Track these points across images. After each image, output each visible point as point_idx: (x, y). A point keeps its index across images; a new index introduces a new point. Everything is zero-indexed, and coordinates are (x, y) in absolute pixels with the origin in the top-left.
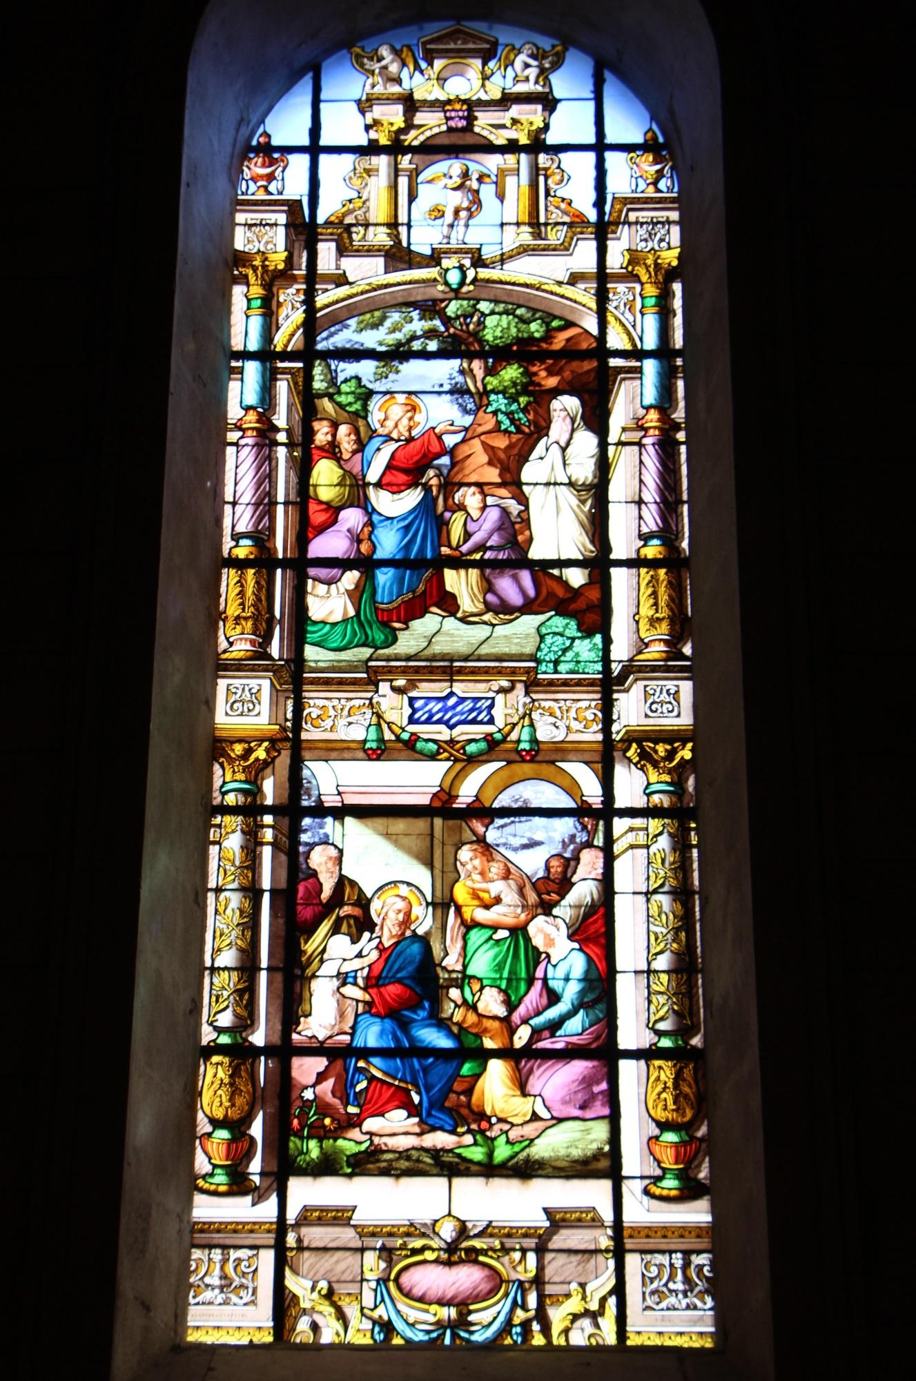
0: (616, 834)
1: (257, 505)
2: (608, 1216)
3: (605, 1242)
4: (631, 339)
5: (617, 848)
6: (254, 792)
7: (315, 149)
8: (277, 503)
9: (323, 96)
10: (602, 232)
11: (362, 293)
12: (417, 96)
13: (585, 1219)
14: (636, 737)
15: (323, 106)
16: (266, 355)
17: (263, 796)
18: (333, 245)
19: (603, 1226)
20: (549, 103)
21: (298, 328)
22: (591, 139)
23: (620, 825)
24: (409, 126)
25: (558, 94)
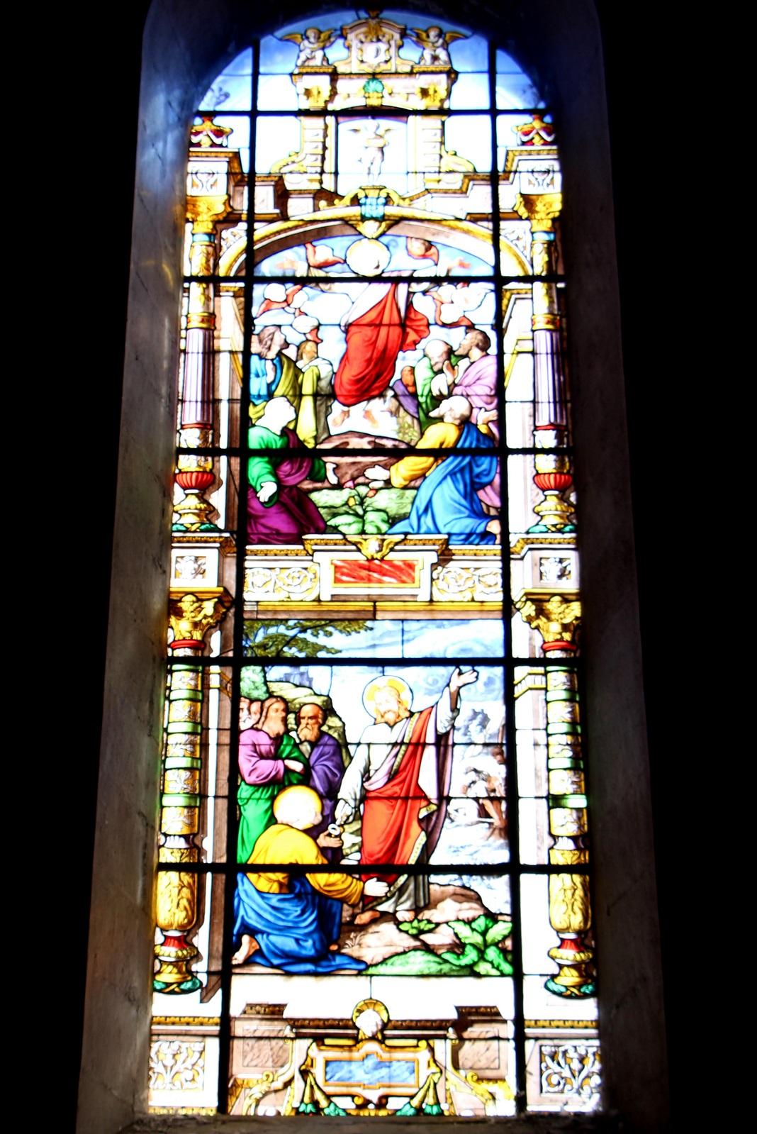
0: (517, 678)
1: (203, 402)
2: (508, 1012)
3: (509, 1030)
4: (521, 263)
5: (517, 691)
6: (202, 645)
7: (254, 114)
8: (219, 401)
9: (262, 70)
10: (494, 179)
11: (296, 227)
12: (340, 70)
13: (491, 1015)
14: (529, 597)
15: (261, 78)
16: (212, 280)
17: (211, 651)
18: (271, 189)
19: (505, 1022)
20: (452, 75)
21: (241, 254)
22: (486, 106)
23: (520, 672)
24: (334, 93)
25: (456, 67)
